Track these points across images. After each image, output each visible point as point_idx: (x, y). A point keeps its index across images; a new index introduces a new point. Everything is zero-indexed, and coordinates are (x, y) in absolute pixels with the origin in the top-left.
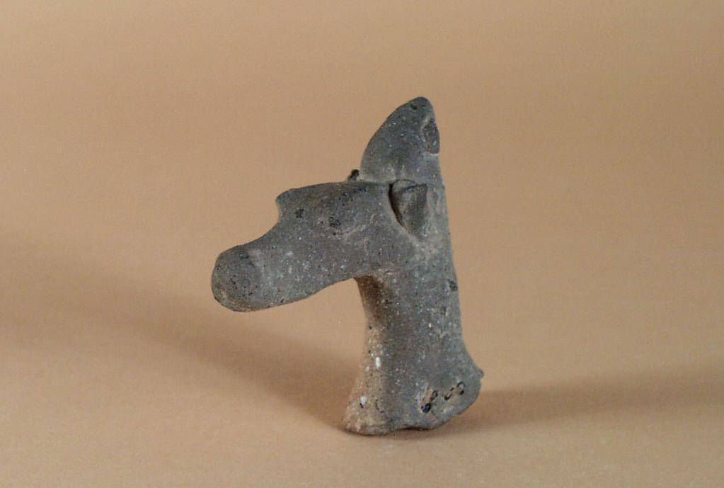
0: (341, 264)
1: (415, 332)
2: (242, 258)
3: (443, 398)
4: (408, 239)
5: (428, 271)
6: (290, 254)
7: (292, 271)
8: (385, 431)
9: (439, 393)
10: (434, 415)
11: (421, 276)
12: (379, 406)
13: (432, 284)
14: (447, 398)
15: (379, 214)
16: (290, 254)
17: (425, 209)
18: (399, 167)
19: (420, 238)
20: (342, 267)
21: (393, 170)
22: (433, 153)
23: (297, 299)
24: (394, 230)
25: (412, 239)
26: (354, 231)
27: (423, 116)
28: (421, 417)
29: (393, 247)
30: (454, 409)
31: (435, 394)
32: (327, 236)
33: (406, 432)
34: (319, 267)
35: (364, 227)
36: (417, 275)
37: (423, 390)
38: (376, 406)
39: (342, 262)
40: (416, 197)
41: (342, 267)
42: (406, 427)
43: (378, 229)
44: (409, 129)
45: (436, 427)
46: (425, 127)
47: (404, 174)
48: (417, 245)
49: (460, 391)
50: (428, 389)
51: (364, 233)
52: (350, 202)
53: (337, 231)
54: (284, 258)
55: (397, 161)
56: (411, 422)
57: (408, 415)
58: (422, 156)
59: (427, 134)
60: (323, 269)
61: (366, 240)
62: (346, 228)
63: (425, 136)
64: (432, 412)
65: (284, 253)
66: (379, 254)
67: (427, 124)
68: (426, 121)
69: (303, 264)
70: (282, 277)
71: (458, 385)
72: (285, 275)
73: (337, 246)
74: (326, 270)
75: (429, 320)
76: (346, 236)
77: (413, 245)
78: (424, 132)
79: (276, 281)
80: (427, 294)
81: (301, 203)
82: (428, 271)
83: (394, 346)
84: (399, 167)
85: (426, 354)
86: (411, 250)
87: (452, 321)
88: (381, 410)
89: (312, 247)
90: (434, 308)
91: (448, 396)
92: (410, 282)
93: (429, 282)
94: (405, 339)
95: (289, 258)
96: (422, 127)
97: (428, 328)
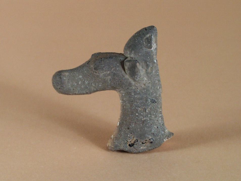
0: (99, 84)
1: (130, 115)
2: (58, 75)
3: (141, 143)
4: (129, 80)
5: (139, 94)
6: (81, 77)
7: (81, 83)
8: (113, 150)
9: (138, 140)
10: (135, 148)
11: (135, 95)
12: (114, 140)
13: (140, 99)
14: (143, 143)
15: (116, 68)
16: (81, 77)
17: (136, 69)
18: (131, 52)
19: (134, 80)
20: (100, 85)
21: (129, 52)
22: (148, 48)
23: (81, 94)
24: (123, 75)
25: (131, 80)
26: (104, 73)
27: (147, 34)
28: (128, 148)
29: (121, 82)
30: (146, 148)
31: (136, 141)
32: (94, 73)
33: (128, 152)
34: (92, 84)
35: (109, 72)
36: (133, 94)
37: (131, 138)
38: (113, 140)
39: (100, 84)
40: (131, 64)
41: (100, 85)
42: (119, 150)
43: (114, 74)
44: (142, 39)
45: (141, 152)
46: (146, 38)
47: (133, 55)
48: (133, 83)
49: (151, 142)
50: (133, 138)
51: (109, 75)
52: (103, 62)
53: (97, 72)
54: (78, 78)
55: (131, 49)
56: (122, 148)
57: (122, 146)
58: (143, 49)
59: (146, 41)
60: (93, 85)
61: (110, 77)
62: (100, 71)
63: (145, 42)
64: (134, 147)
65: (78, 76)
66: (114, 83)
67: (148, 37)
68: (148, 36)
69: (86, 82)
70: (76, 84)
71: (150, 139)
72: (77, 84)
73: (98, 77)
74: (94, 85)
75: (137, 112)
76: (102, 74)
77: (131, 83)
78: (145, 40)
79: (72, 86)
80: (137, 102)
81: (100, 59)
82: (139, 94)
83: (123, 119)
84: (131, 52)
85: (134, 125)
86: (130, 84)
87: (150, 114)
88: (114, 142)
89: (89, 76)
90: (140, 108)
91: (144, 143)
92: (130, 96)
93: (139, 98)
94: (126, 117)
95: (80, 79)
96: (145, 38)
97: (136, 115)
